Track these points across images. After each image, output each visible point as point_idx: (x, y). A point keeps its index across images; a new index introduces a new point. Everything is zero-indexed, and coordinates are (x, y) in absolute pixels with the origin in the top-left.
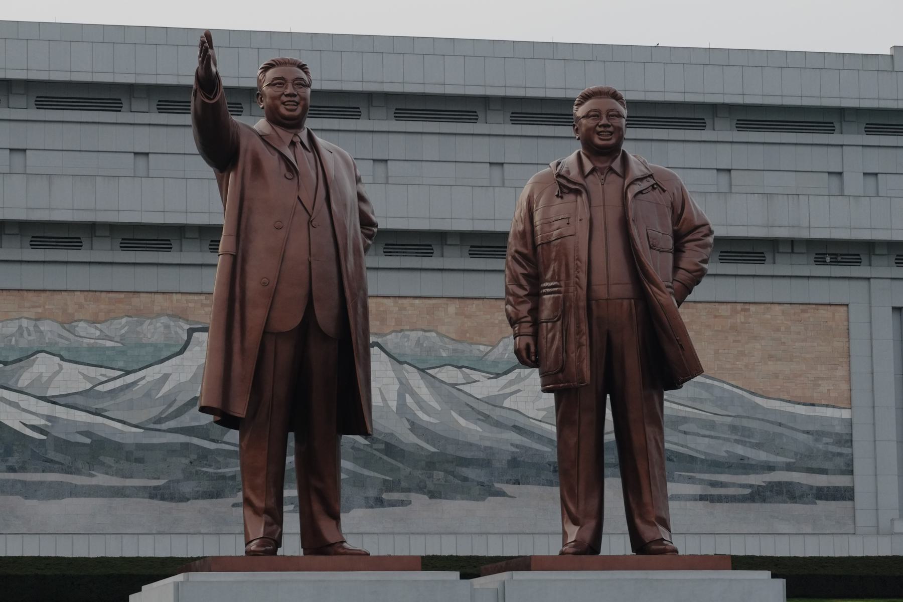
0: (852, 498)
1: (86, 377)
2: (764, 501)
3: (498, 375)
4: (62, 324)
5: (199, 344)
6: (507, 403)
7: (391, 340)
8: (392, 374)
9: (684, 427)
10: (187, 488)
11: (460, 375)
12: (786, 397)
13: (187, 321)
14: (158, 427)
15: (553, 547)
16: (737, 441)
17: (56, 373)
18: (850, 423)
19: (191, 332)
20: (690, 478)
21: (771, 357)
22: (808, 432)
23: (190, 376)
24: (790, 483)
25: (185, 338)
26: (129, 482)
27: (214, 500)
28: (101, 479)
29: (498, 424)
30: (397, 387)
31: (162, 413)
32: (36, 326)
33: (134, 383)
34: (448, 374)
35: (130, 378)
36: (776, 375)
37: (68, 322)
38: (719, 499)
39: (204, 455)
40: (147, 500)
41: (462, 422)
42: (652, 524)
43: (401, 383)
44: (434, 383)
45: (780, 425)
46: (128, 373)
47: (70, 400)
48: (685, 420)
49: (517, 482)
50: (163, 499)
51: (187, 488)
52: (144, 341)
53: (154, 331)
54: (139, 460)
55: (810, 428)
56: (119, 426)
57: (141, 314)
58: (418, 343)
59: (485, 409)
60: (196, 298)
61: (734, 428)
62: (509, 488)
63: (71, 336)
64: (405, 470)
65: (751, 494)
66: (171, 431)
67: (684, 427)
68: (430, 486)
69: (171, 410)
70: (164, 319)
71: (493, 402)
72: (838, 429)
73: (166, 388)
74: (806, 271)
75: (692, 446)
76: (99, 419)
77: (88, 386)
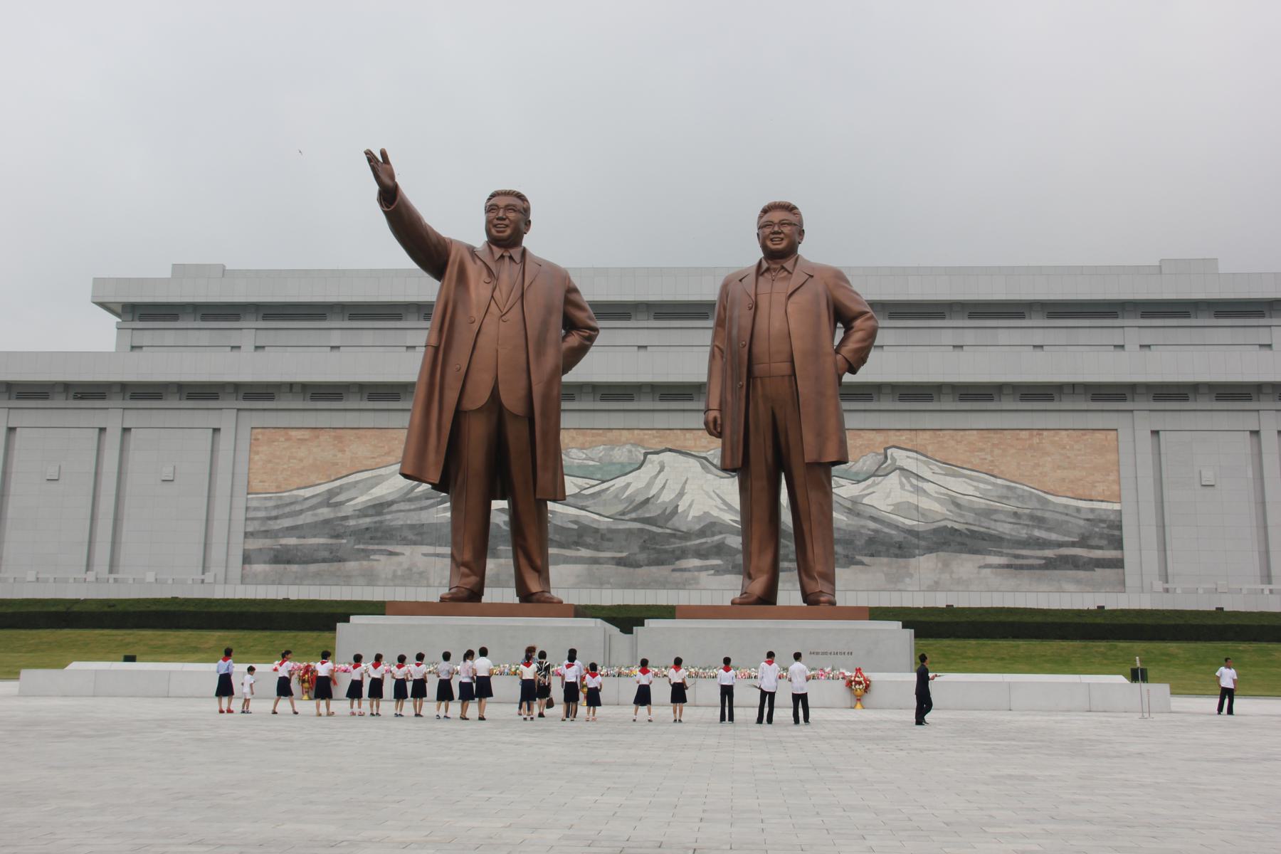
0: (1122, 567)
2: (1055, 568)
3: (859, 482)
5: (652, 462)
6: (865, 501)
9: (994, 517)
10: (642, 557)
13: (643, 447)
15: (433, 595)
16: (1033, 527)
18: (1120, 512)
19: (646, 454)
21: (1059, 467)
26: (602, 555)
28: (584, 553)
29: (858, 515)
35: (605, 486)
36: (1063, 480)
38: (1021, 567)
39: (653, 536)
42: (813, 578)
48: (996, 511)
49: (872, 555)
50: (625, 565)
51: (642, 557)
53: (620, 455)
54: (610, 540)
55: (1091, 516)
56: (596, 517)
57: (613, 444)
59: (849, 504)
61: (1032, 517)
62: (866, 560)
67: (994, 517)
70: (628, 447)
71: (855, 501)
72: (1112, 517)
74: (1084, 406)
76: (583, 513)
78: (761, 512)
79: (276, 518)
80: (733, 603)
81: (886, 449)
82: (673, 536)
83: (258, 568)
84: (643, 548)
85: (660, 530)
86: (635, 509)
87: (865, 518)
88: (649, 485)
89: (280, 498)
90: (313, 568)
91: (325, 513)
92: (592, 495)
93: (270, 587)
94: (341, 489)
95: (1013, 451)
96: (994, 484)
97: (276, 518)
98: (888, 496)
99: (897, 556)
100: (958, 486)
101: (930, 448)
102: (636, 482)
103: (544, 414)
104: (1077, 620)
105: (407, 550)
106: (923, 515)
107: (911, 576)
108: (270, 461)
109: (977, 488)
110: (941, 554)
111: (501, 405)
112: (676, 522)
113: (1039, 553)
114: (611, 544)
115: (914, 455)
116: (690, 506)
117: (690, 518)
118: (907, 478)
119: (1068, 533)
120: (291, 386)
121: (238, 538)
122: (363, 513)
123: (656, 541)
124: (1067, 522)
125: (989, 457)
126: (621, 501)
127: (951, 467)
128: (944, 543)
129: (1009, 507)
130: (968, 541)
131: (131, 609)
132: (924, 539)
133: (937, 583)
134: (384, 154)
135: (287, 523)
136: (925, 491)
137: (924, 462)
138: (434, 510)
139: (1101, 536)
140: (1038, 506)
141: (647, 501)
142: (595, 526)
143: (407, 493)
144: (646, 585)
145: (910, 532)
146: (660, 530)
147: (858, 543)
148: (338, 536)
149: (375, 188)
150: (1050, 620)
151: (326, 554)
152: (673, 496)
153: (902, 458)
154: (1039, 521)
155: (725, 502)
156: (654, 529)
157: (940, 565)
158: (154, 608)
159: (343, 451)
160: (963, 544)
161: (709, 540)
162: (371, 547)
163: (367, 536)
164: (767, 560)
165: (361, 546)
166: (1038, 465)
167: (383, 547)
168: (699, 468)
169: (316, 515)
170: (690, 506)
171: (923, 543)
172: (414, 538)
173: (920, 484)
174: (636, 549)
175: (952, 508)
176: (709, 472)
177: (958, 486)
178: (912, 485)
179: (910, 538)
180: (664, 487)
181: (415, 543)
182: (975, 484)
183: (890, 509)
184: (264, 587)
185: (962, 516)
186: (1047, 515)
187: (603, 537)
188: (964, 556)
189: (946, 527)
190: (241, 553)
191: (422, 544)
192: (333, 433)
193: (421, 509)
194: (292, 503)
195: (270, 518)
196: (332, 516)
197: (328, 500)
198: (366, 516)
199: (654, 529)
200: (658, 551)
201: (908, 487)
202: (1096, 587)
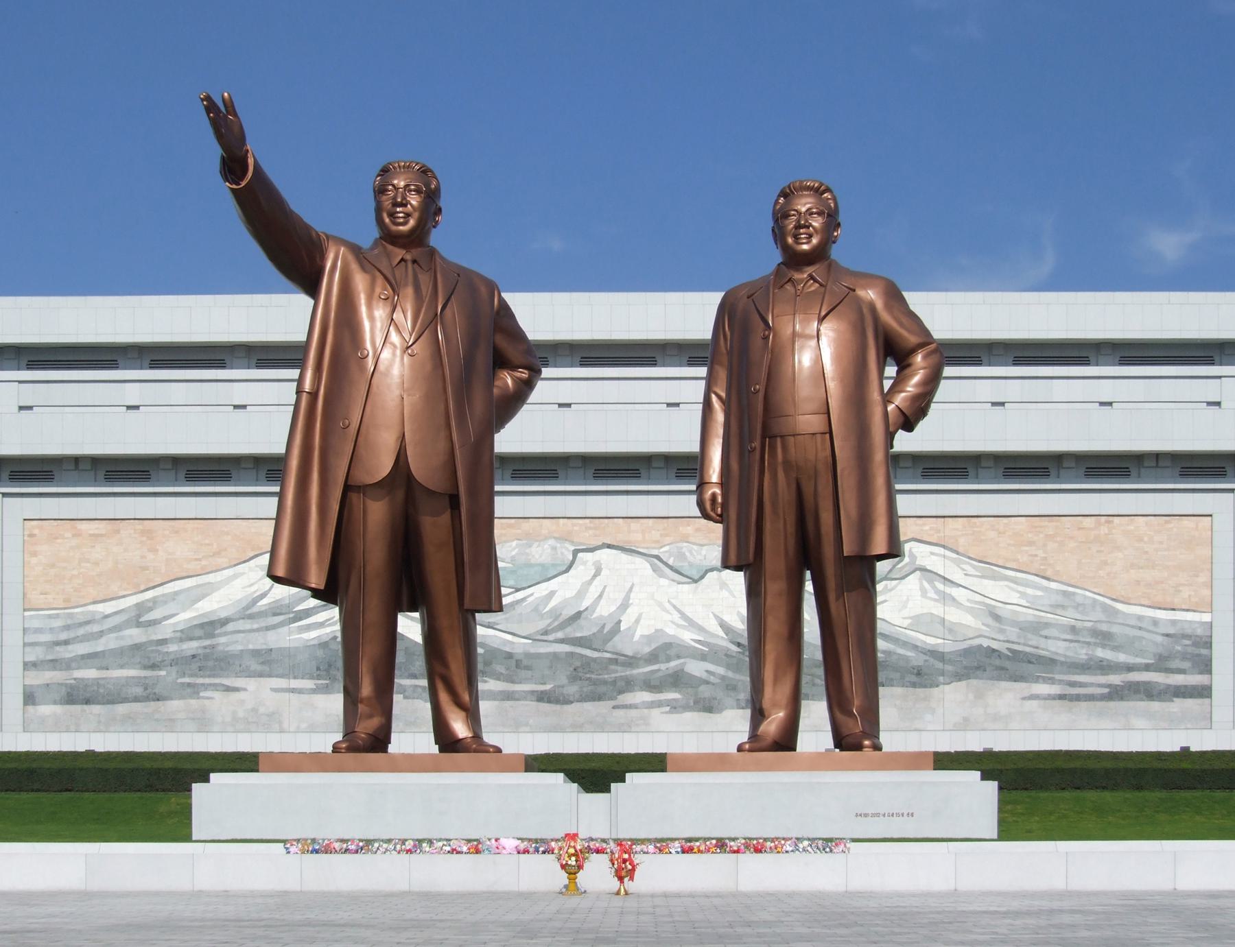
5: (585, 563)
9: (1044, 633)
10: (572, 690)
12: (1146, 603)
13: (572, 543)
16: (1096, 644)
19: (575, 553)
20: (1050, 679)
22: (1167, 635)
23: (574, 592)
24: (1149, 683)
27: (596, 703)
31: (549, 625)
33: (524, 599)
35: (520, 595)
39: (587, 663)
40: (535, 703)
45: (1140, 628)
46: (518, 590)
48: (1047, 625)
50: (549, 702)
51: (572, 690)
52: (533, 561)
54: (528, 668)
55: (1171, 631)
56: (509, 637)
60: (580, 521)
61: (1095, 633)
65: (1109, 693)
66: (562, 641)
69: (556, 624)
70: (551, 542)
72: (1199, 632)
75: (1053, 649)
79: (66, 643)
82: (615, 662)
83: (46, 710)
84: (574, 679)
85: (595, 655)
86: (562, 627)
88: (581, 594)
90: (121, 709)
91: (134, 635)
93: (65, 735)
96: (1046, 589)
97: (66, 643)
98: (905, 606)
99: (914, 685)
100: (1000, 592)
102: (563, 590)
103: (473, 492)
105: (251, 684)
106: (951, 631)
109: (1023, 595)
110: (974, 682)
111: (409, 476)
112: (618, 644)
113: (1102, 679)
116: (637, 621)
117: (636, 638)
118: (931, 582)
119: (1140, 653)
122: (186, 635)
123: (594, 668)
124: (1141, 638)
126: (542, 616)
127: (989, 566)
128: (978, 668)
129: (1067, 618)
130: (1007, 664)
132: (950, 662)
136: (954, 599)
137: (952, 560)
138: (286, 629)
139: (1184, 656)
140: (1102, 617)
141: (578, 615)
142: (508, 649)
143: (247, 608)
144: (577, 728)
145: (934, 653)
146: (595, 655)
148: (153, 667)
150: (1121, 765)
151: (139, 691)
152: (613, 608)
154: (1104, 638)
155: (684, 616)
156: (588, 653)
160: (1002, 668)
161: (663, 667)
162: (200, 681)
163: (195, 666)
165: (187, 680)
167: (217, 681)
168: (649, 571)
169: (122, 638)
170: (637, 621)
171: (949, 668)
172: (259, 668)
174: (564, 680)
175: (990, 621)
176: (662, 575)
177: (1000, 592)
178: (937, 591)
179: (932, 660)
180: (600, 596)
181: (261, 675)
182: (1021, 589)
183: (906, 623)
185: (1002, 631)
186: (1115, 629)
187: (518, 664)
188: (1004, 684)
190: (21, 690)
191: (270, 676)
193: (268, 628)
194: (88, 623)
195: (57, 643)
196: (144, 639)
197: (138, 617)
198: (191, 639)
199: (588, 653)
200: (595, 683)
201: (932, 594)
202: (1173, 723)
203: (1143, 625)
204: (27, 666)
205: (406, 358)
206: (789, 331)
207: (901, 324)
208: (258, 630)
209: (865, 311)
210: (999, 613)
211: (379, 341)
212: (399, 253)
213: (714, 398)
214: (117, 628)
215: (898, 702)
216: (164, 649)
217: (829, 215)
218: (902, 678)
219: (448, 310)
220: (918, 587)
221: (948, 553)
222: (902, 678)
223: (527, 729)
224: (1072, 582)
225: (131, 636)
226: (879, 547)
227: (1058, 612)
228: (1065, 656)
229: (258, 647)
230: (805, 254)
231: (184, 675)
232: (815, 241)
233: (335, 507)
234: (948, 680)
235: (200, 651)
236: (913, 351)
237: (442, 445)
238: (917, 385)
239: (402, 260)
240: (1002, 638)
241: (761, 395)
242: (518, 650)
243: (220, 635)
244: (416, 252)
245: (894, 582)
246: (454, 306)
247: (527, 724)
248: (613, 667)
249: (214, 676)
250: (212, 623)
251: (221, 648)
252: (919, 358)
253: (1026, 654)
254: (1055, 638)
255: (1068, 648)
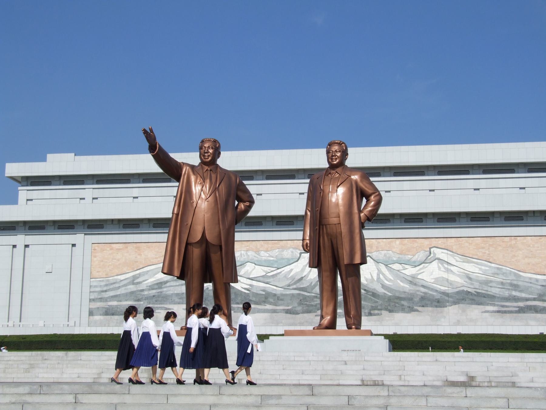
1: (264, 271)
2: (524, 313)
3: (416, 266)
4: (255, 252)
5: (304, 258)
6: (419, 277)
7: (375, 255)
8: (375, 267)
9: (490, 285)
10: (299, 309)
11: (401, 267)
12: (533, 272)
14: (289, 288)
16: (512, 289)
17: (253, 269)
21: (526, 257)
22: (543, 286)
24: (535, 306)
25: (299, 256)
26: (278, 308)
28: (268, 307)
29: (415, 284)
30: (377, 271)
32: (246, 253)
33: (281, 272)
34: (396, 266)
35: (279, 271)
36: (529, 264)
37: (257, 252)
38: (505, 312)
39: (305, 298)
40: (284, 314)
41: (402, 284)
43: (378, 270)
44: (391, 270)
45: (531, 283)
46: (278, 269)
47: (258, 279)
48: (491, 281)
49: (423, 306)
50: (290, 313)
51: (299, 309)
53: (287, 254)
54: (282, 300)
56: (275, 288)
57: (283, 248)
58: (385, 255)
59: (410, 279)
61: (511, 285)
62: (420, 309)
63: (259, 257)
64: (380, 302)
67: (490, 285)
68: (389, 308)
70: (291, 249)
73: (292, 274)
76: (268, 285)
77: (264, 274)
78: (327, 287)
79: (106, 291)
80: (314, 329)
81: (430, 248)
83: (97, 318)
84: (300, 304)
85: (308, 294)
86: (295, 283)
87: (419, 286)
89: (108, 280)
91: (132, 288)
92: (273, 276)
93: (103, 328)
94: (140, 275)
95: (500, 248)
96: (490, 267)
97: (106, 291)
98: (432, 274)
99: (436, 307)
100: (471, 268)
101: (454, 247)
104: (524, 340)
106: (451, 284)
107: (445, 317)
108: (102, 261)
109: (480, 269)
110: (461, 305)
113: (516, 304)
114: (282, 302)
115: (446, 251)
118: (442, 264)
120: (112, 221)
121: (86, 302)
122: (151, 288)
124: (531, 287)
125: (487, 252)
128: (463, 299)
129: (499, 279)
130: (475, 298)
131: (34, 340)
132: (451, 297)
133: (458, 321)
134: (151, 130)
135: (111, 294)
136: (452, 271)
137: (451, 255)
140: (514, 278)
141: (302, 278)
145: (444, 293)
146: (308, 294)
147: (415, 300)
148: (138, 300)
149: (147, 145)
153: (439, 253)
154: (516, 287)
157: (460, 311)
158: (45, 339)
159: (140, 255)
160: (473, 300)
163: (154, 300)
164: (330, 308)
166: (514, 256)
167: (162, 306)
169: (127, 289)
171: (451, 299)
173: (450, 267)
174: (296, 305)
175: (467, 280)
177: (471, 268)
178: (445, 268)
179: (444, 296)
181: (179, 303)
182: (480, 267)
183: (433, 280)
184: (100, 328)
185: (472, 284)
186: (520, 283)
188: (473, 306)
189: (463, 291)
192: (135, 245)
194: (114, 283)
196: (135, 289)
197: (133, 281)
198: (153, 289)
200: (308, 306)
201: (443, 269)
203: (532, 282)
204: (91, 300)
205: (206, 203)
206: (328, 191)
207: (366, 187)
208: (178, 286)
209: (353, 183)
210: (471, 276)
211: (198, 196)
212: (206, 168)
213: (308, 211)
214: (125, 285)
215: (430, 314)
216: (143, 293)
217: (343, 152)
218: (432, 303)
219: (220, 186)
220: (437, 266)
221: (449, 252)
222: (432, 303)
223: (282, 324)
224: (501, 264)
225: (130, 288)
226: (357, 260)
227: (496, 276)
228: (499, 294)
229: (178, 292)
230: (335, 164)
231: (150, 303)
232: (337, 161)
233: (183, 250)
234: (450, 304)
235: (156, 294)
236: (370, 195)
237: (217, 230)
238: (371, 207)
239: (207, 170)
240: (472, 287)
241: (319, 211)
242: (278, 293)
243: (164, 288)
244: (211, 167)
245: (427, 264)
246: (222, 184)
247: (281, 323)
248: (315, 299)
249: (161, 304)
250: (161, 283)
251: (164, 293)
252: (372, 197)
253: (483, 293)
254: (494, 287)
255: (500, 291)
